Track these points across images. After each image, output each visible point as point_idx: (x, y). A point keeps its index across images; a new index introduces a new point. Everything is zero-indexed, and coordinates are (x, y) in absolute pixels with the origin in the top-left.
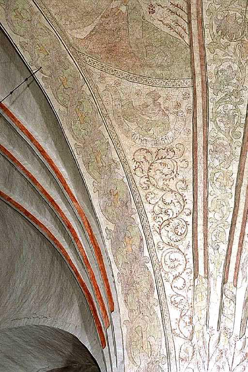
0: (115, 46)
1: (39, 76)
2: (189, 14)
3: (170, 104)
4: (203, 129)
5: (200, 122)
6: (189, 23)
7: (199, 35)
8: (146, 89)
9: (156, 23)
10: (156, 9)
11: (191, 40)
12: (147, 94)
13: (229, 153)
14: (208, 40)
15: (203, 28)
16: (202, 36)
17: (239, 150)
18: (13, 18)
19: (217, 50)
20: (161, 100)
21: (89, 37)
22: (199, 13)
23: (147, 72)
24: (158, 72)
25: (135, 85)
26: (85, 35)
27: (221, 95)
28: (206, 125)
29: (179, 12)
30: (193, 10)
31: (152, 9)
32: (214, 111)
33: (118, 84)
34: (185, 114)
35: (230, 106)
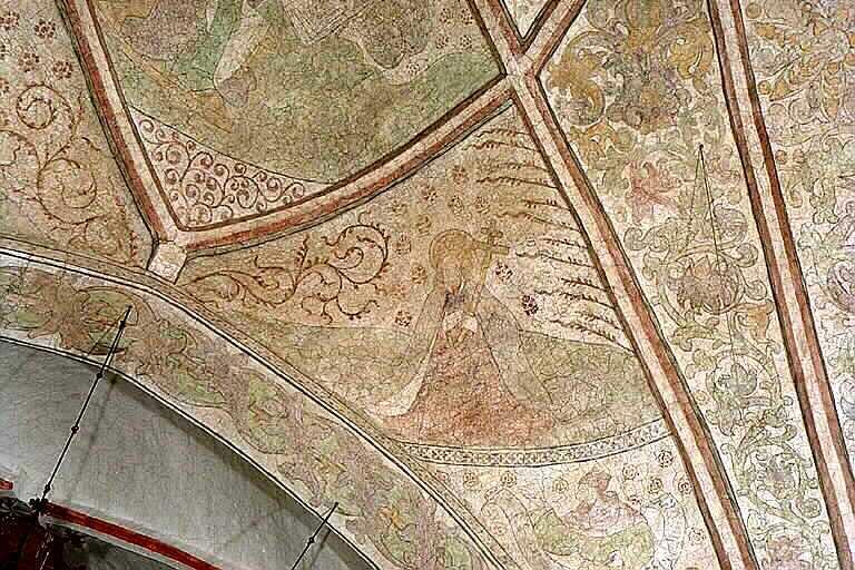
0: (478, 404)
1: (336, 522)
2: (607, 289)
3: (639, 487)
4: (729, 519)
5: (716, 509)
6: (615, 307)
7: (644, 325)
8: (574, 472)
9: (548, 328)
10: (539, 300)
11: (632, 339)
12: (580, 483)
13: (807, 556)
14: (667, 327)
15: (647, 307)
16: (650, 324)
17: (828, 540)
18: (251, 424)
19: (697, 342)
20: (614, 485)
21: (418, 406)
22: (629, 279)
23: (564, 435)
24: (588, 426)
25: (547, 470)
26: (407, 403)
27: (740, 432)
28: (731, 505)
30: (613, 279)
31: (530, 305)
32: (738, 473)
33: (508, 481)
34: (679, 497)
35: (775, 450)
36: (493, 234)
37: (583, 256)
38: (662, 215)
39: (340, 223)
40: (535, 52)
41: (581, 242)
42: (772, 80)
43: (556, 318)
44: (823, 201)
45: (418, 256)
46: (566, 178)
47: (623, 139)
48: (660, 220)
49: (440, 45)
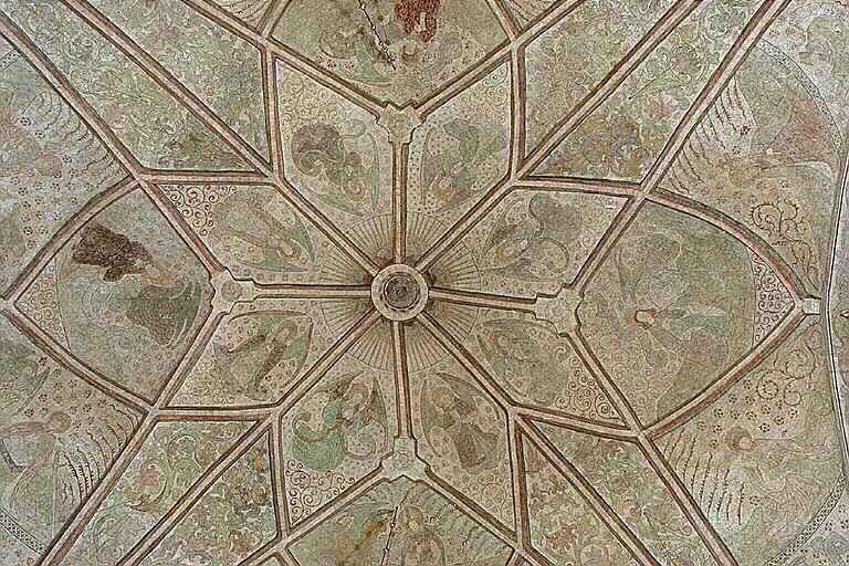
8: (807, 70)
14: (713, 68)
20: (803, 49)
23: (794, 84)
29: (720, 110)
36: (721, 165)
37: (706, 121)
38: (668, 98)
39: (760, 232)
40: (629, 192)
41: (700, 126)
42: (586, 86)
43: (742, 115)
44: (620, 35)
45: (752, 189)
46: (673, 150)
47: (646, 133)
48: (670, 97)
49: (654, 229)
